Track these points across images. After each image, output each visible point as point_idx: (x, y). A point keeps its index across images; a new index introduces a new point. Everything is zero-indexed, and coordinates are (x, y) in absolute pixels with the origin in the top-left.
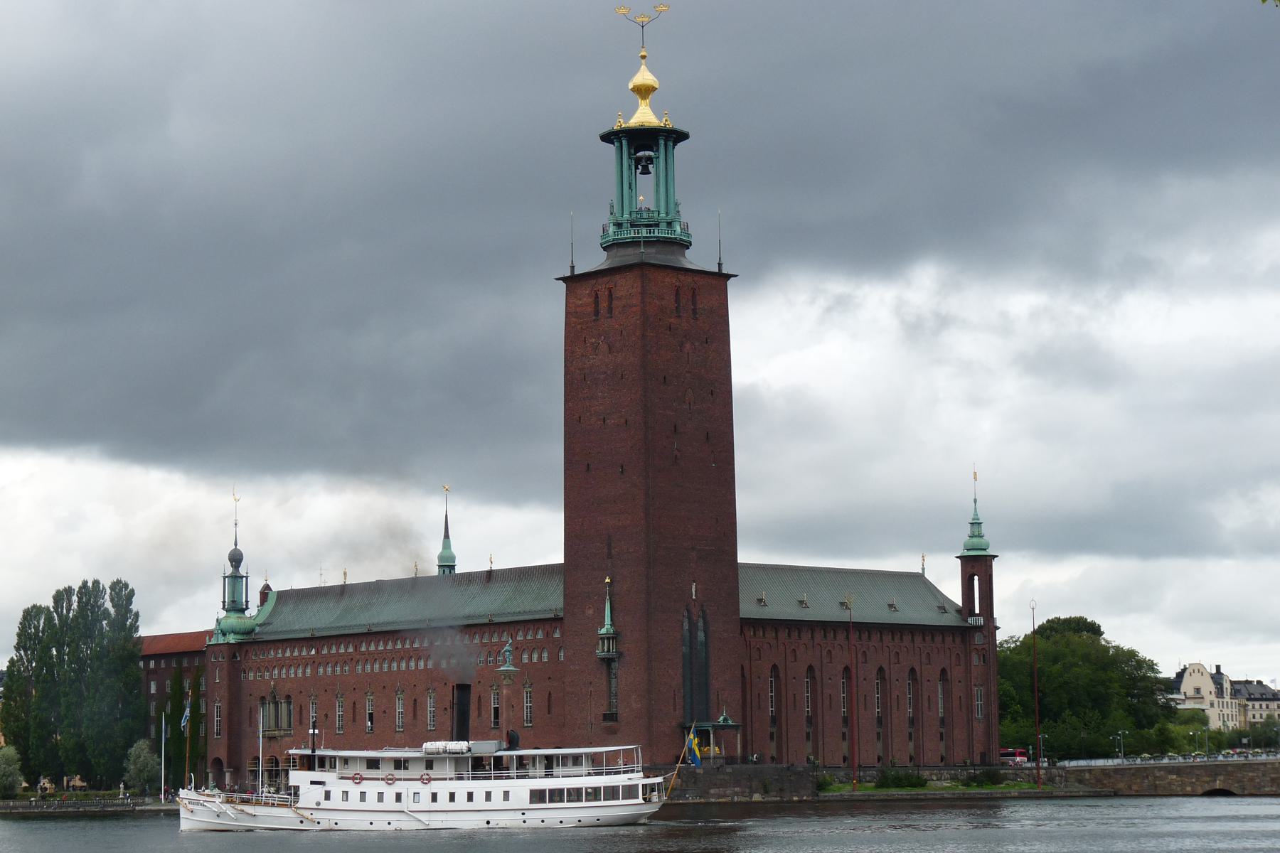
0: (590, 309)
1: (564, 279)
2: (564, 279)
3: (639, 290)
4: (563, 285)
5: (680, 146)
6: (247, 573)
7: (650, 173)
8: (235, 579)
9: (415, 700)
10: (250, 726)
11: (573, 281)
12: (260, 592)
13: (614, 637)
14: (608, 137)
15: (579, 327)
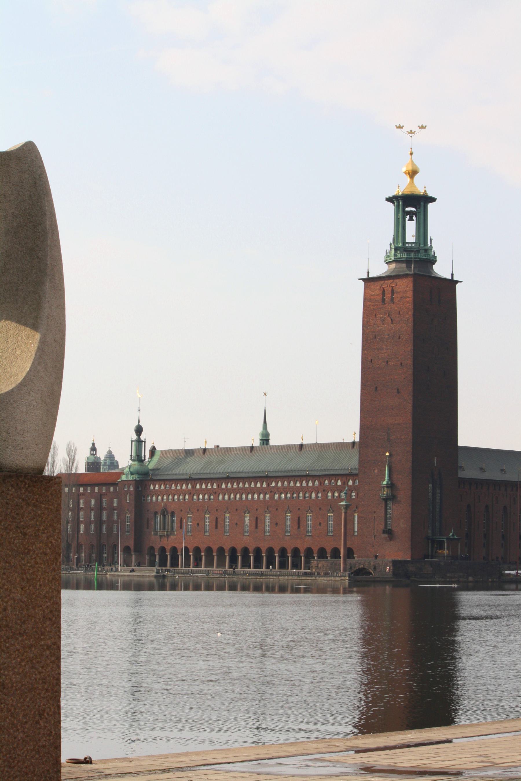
0: (380, 298)
1: (363, 280)
2: (363, 280)
3: (411, 288)
4: (362, 283)
5: (431, 206)
6: (145, 439)
7: (413, 220)
8: (139, 442)
9: (257, 518)
10: (148, 528)
11: (368, 281)
12: (150, 451)
13: (391, 486)
14: (389, 200)
15: (372, 307)
